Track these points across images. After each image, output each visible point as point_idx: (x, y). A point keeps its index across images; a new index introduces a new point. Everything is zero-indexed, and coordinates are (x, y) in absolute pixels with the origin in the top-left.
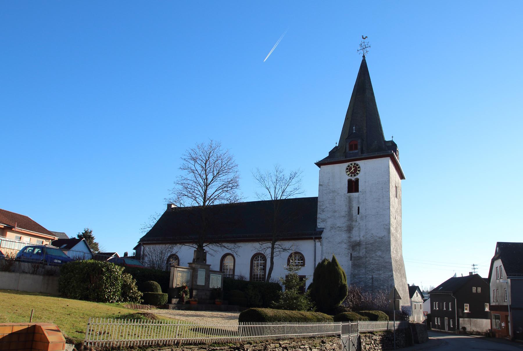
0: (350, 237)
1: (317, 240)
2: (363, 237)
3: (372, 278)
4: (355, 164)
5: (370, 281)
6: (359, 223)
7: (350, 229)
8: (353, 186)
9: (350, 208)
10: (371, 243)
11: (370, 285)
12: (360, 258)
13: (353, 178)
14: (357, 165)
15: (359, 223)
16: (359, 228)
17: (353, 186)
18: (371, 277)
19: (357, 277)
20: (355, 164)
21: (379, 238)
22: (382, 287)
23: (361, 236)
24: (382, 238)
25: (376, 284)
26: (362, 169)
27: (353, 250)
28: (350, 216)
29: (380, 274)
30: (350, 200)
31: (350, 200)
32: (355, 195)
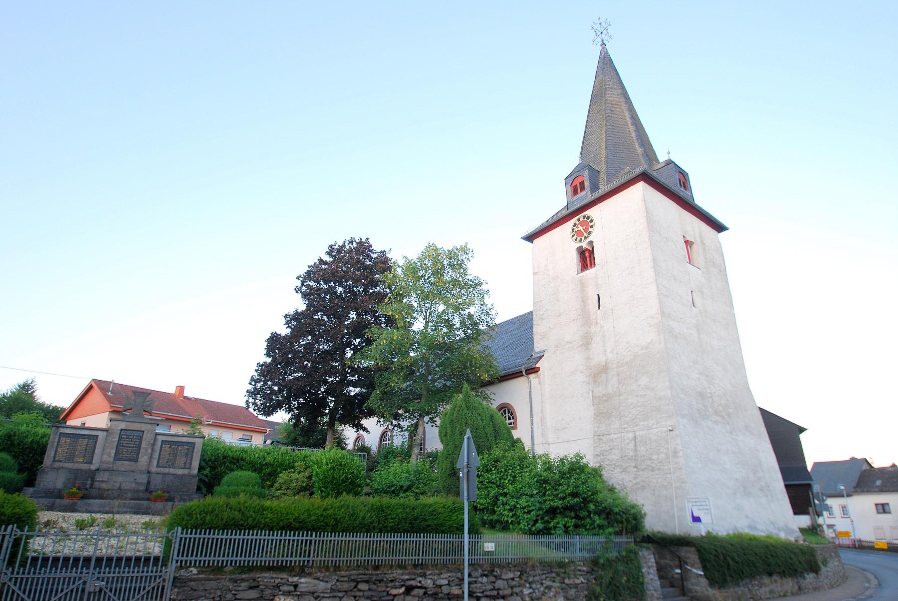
0: (588, 358)
1: (532, 376)
2: (612, 352)
3: (635, 438)
4: (584, 217)
5: (631, 446)
6: (602, 327)
7: (586, 342)
8: (586, 258)
9: (584, 301)
10: (627, 362)
11: (632, 453)
12: (607, 398)
13: (584, 245)
14: (588, 218)
15: (602, 327)
16: (604, 336)
17: (586, 258)
18: (631, 435)
19: (604, 439)
20: (584, 217)
21: (642, 348)
22: (655, 457)
23: (608, 351)
24: (647, 348)
25: (642, 450)
26: (597, 223)
27: (595, 382)
28: (585, 318)
29: (649, 428)
30: (583, 286)
31: (583, 286)
32: (590, 272)
